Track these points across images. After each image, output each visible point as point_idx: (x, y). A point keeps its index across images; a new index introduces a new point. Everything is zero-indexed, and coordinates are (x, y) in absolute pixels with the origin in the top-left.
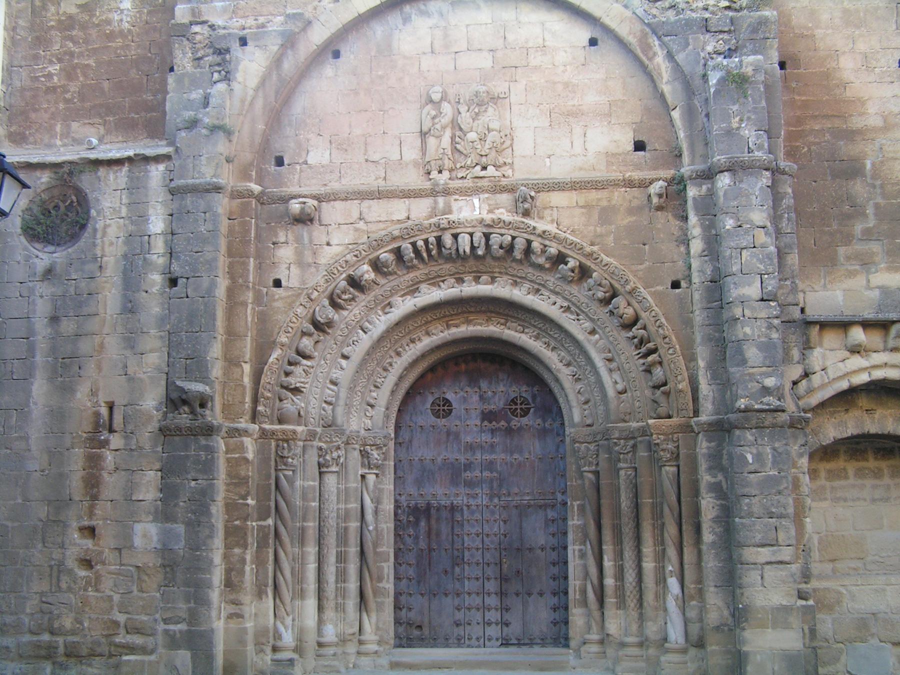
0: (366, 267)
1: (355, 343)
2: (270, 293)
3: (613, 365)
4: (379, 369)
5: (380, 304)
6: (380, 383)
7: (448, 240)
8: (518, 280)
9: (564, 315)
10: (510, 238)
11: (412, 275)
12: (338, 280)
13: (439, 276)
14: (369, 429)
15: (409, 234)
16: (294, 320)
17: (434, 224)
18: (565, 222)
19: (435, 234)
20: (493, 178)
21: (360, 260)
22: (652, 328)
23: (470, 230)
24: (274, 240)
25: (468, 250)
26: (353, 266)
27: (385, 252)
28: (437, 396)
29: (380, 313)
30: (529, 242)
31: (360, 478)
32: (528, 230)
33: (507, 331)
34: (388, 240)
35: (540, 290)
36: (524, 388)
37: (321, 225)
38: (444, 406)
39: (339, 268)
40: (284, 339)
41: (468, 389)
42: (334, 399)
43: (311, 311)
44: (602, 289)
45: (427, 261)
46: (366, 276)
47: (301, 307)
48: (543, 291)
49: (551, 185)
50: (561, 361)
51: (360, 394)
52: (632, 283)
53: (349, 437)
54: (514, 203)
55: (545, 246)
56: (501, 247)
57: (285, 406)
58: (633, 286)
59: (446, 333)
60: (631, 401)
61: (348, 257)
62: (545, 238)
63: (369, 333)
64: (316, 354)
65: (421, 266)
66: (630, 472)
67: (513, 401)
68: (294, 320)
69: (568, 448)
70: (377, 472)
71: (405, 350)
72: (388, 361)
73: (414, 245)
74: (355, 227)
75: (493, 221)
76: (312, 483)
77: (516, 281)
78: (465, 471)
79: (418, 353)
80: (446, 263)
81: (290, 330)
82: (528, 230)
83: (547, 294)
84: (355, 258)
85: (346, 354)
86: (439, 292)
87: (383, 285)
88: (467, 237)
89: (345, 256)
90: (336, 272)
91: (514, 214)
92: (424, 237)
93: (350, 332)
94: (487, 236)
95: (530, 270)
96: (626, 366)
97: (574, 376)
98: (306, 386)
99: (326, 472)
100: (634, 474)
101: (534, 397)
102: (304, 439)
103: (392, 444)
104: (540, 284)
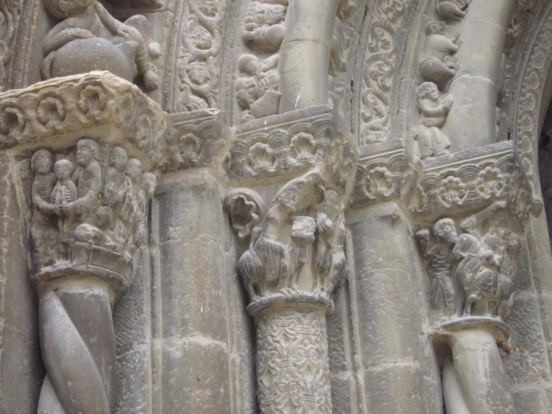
42: (282, 26)
51: (387, 37)
53: (360, 173)
57: (70, 31)
76: (204, 341)
99: (271, 305)
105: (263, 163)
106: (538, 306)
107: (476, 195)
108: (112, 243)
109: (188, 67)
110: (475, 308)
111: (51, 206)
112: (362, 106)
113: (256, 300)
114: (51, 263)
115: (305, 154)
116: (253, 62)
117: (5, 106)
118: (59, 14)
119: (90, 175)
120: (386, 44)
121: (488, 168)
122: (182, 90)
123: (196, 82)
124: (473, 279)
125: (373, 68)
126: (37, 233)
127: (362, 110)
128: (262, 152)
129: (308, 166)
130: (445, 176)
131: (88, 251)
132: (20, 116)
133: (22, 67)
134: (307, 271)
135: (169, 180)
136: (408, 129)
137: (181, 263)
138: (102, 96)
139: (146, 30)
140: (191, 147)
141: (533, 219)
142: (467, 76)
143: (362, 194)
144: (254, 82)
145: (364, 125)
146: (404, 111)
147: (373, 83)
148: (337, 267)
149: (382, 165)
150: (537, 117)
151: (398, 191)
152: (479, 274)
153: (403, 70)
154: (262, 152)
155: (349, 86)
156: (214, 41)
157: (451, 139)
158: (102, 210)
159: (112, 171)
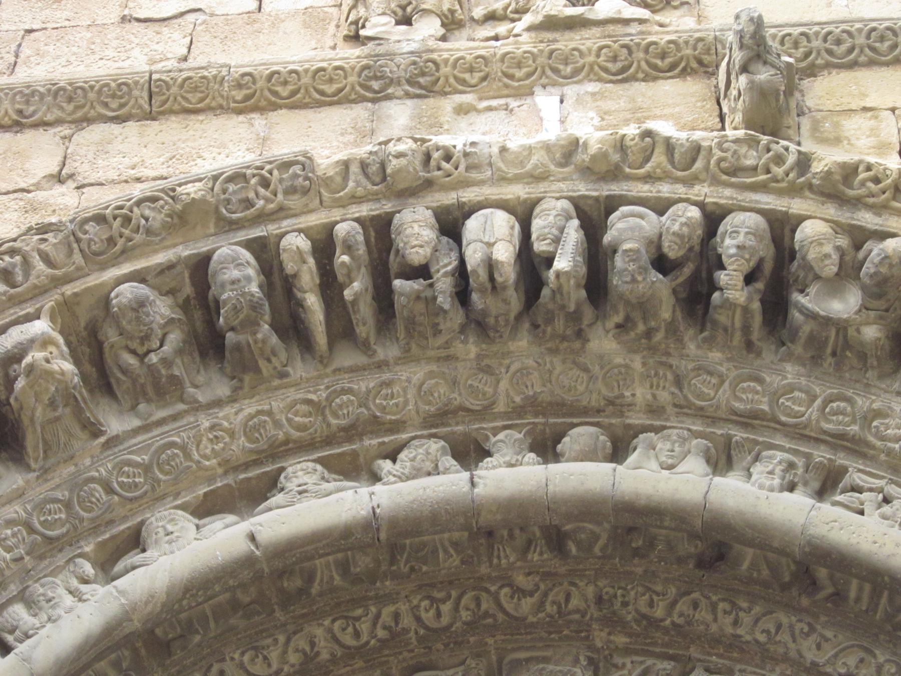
5: (96, 529)
8: (739, 434)
10: (694, 213)
11: (249, 407)
13: (376, 425)
15: (248, 204)
19: (364, 210)
20: (619, 29)
21: (18, 301)
23: (517, 192)
29: (88, 569)
32: (779, 171)
34: (157, 218)
35: (844, 470)
46: (35, 356)
49: (861, 40)
54: (711, 105)
62: (856, 203)
63: (21, 648)
65: (299, 370)
74: (30, 202)
77: (729, 438)
80: (406, 358)
92: (314, 220)
95: (792, 373)
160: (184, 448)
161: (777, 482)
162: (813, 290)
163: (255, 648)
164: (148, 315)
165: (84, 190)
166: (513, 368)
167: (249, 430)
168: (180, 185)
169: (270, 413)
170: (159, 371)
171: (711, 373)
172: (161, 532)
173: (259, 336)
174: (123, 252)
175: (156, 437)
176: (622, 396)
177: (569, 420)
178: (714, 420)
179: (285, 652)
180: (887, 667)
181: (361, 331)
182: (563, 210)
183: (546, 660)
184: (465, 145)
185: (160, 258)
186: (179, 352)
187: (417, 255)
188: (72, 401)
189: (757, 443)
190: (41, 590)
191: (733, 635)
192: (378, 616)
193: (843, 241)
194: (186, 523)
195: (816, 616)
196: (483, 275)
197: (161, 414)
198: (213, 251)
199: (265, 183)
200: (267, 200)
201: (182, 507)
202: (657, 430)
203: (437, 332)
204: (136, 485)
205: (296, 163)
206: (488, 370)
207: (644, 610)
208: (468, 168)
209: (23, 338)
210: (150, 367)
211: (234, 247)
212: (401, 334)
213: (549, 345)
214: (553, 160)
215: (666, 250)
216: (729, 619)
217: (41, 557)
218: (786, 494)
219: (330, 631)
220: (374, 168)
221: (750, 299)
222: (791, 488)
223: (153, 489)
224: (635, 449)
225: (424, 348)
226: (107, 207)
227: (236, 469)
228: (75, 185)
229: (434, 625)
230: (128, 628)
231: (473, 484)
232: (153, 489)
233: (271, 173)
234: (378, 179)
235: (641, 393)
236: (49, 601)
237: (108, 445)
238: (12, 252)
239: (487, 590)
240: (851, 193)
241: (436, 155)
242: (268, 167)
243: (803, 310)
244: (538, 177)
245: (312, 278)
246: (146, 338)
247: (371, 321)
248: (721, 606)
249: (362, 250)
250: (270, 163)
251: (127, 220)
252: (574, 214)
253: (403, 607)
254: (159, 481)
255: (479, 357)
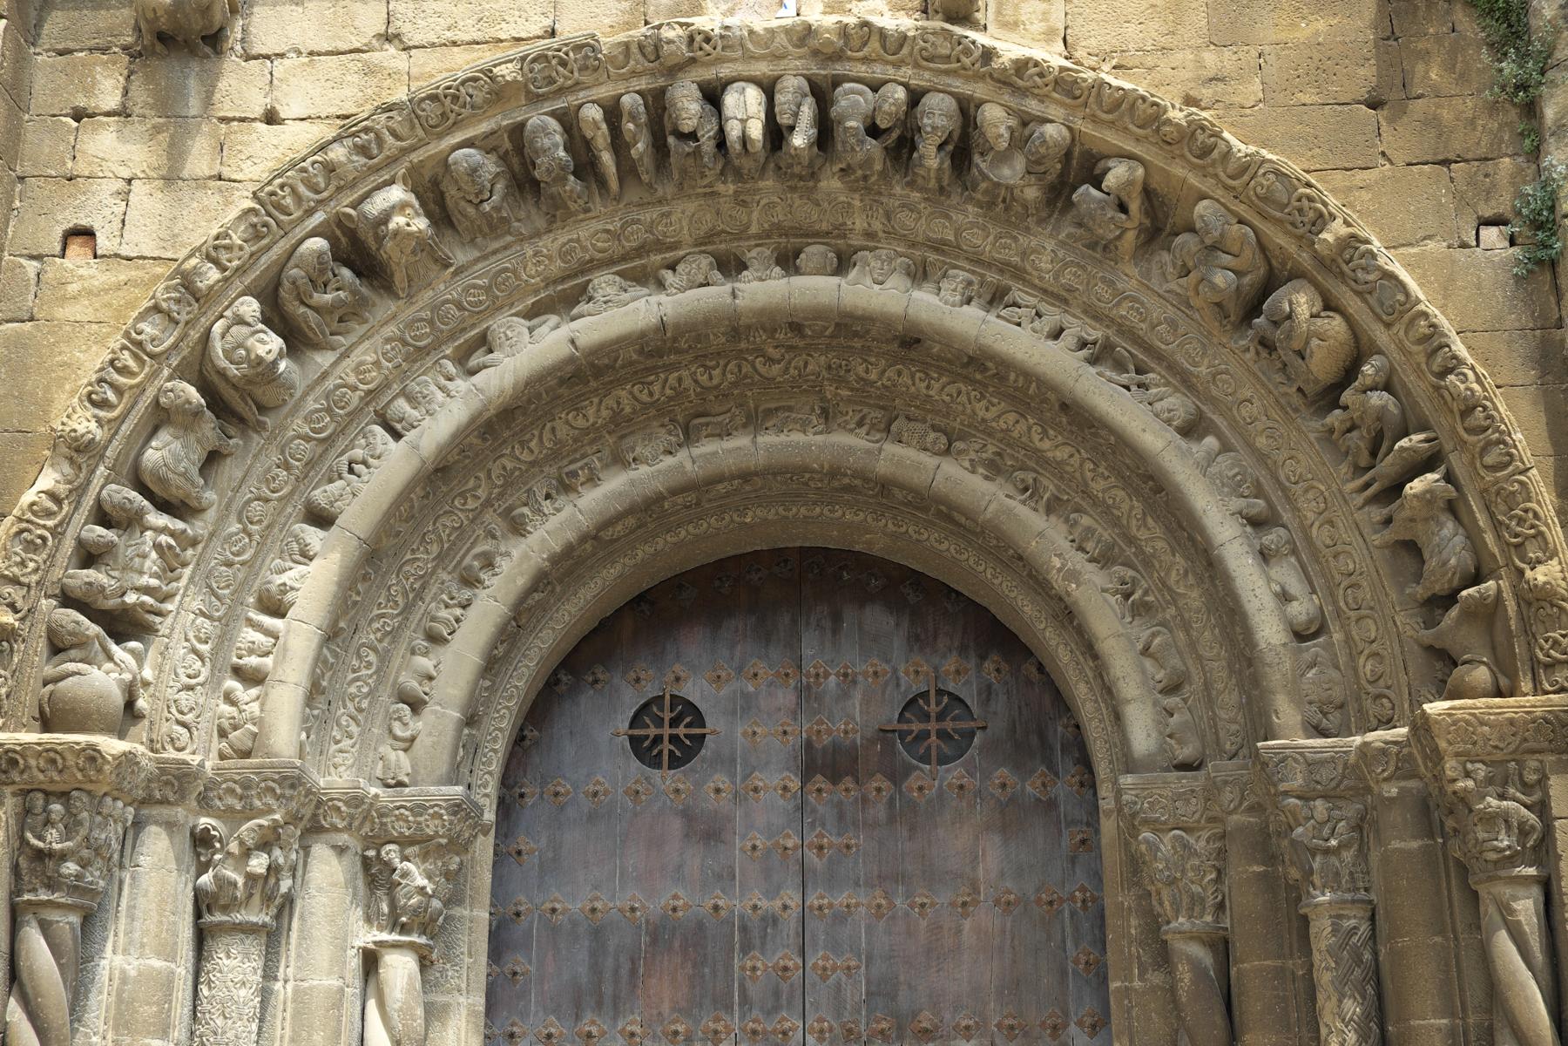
0: (396, 193)
1: (358, 468)
2: (49, 276)
3: (1272, 537)
4: (445, 576)
5: (452, 336)
6: (446, 622)
7: (688, 106)
8: (932, 257)
9: (1092, 370)
10: (901, 94)
12: (299, 232)
14: (400, 784)
15: (552, 81)
16: (127, 359)
17: (641, 47)
18: (1090, 40)
19: (643, 84)
21: (376, 169)
22: (1419, 387)
23: (762, 69)
24: (81, 102)
25: (756, 130)
26: (353, 185)
27: (468, 143)
28: (651, 691)
29: (450, 367)
30: (967, 110)
31: (354, 963)
32: (967, 61)
33: (891, 449)
34: (479, 97)
35: (1007, 290)
36: (950, 664)
37: (248, 58)
38: (674, 722)
39: (302, 189)
40: (85, 424)
41: (762, 668)
42: (268, 661)
43: (195, 335)
44: (1226, 259)
45: (614, 184)
46: (398, 221)
47: (157, 318)
48: (1017, 294)
50: (1081, 549)
51: (372, 657)
52: (1339, 221)
55: (1026, 121)
56: (873, 131)
58: (1344, 231)
59: (682, 455)
60: (1342, 660)
61: (338, 153)
62: (1024, 92)
63: (410, 436)
64: (210, 495)
65: (598, 206)
66: (1353, 922)
67: (911, 703)
68: (127, 359)
69: (1112, 857)
70: (423, 940)
71: (539, 511)
72: (478, 549)
73: (569, 121)
74: (366, 63)
75: (844, 30)
76: (157, 963)
78: (746, 949)
79: (585, 522)
81: (111, 396)
82: (967, 61)
83: (1032, 301)
84: (361, 160)
85: (323, 502)
86: (662, 298)
87: (459, 271)
88: (754, 96)
89: (322, 148)
90: (289, 201)
91: (917, 15)
92: (605, 91)
93: (342, 431)
94: (822, 93)
96: (1320, 535)
97: (1127, 596)
98: (169, 606)
100: (1364, 928)
101: (987, 693)
102: (141, 793)
103: (484, 848)
104: (1004, 267)
105: (230, 801)
106: (468, 924)
107: (422, 830)
108: (90, 879)
109: (176, 697)
110: (404, 929)
111: (41, 844)
112: (335, 728)
113: (208, 918)
114: (34, 890)
115: (270, 801)
116: (238, 693)
117: (7, 751)
118: (61, 645)
119: (80, 823)
120: (369, 664)
121: (436, 809)
122: (167, 720)
123: (182, 713)
124: (406, 904)
125: (353, 690)
126: (23, 863)
127: (334, 733)
128: (231, 791)
129: (271, 811)
130: (398, 808)
131: (69, 887)
132: (21, 762)
133: (22, 699)
134: (256, 899)
135: (145, 812)
136: (375, 749)
137: (147, 891)
138: (100, 761)
139: (139, 658)
140: (169, 787)
141: (481, 838)
142: (438, 708)
143: (319, 822)
144: (236, 714)
145: (334, 747)
146: (375, 731)
147: (350, 705)
148: (282, 896)
149: (340, 800)
150: (507, 733)
151: (350, 825)
152: (412, 901)
153: (381, 688)
154: (231, 791)
155: (326, 707)
156: (203, 669)
157: (412, 767)
158: (85, 853)
159: (99, 819)
160: (514, 272)
161: (958, 298)
162: (989, 158)
163: (577, 409)
164: (480, 177)
165: (413, 52)
166: (763, 202)
167: (563, 255)
168: (495, 66)
169: (578, 240)
170: (491, 216)
171: (912, 211)
172: (504, 338)
173: (567, 188)
174: (454, 124)
175: (493, 264)
176: (845, 224)
177: (805, 240)
178: (913, 245)
179: (598, 410)
180: (1035, 428)
181: (645, 178)
182: (799, 88)
183: (790, 409)
184: (721, 28)
185: (484, 127)
186: (504, 198)
187: (687, 126)
188: (428, 248)
189: (946, 263)
190: (418, 389)
191: (927, 396)
192: (666, 380)
193: (1013, 122)
194: (521, 325)
195: (985, 386)
196: (738, 147)
197: (496, 245)
198: (527, 120)
199: (563, 64)
200: (566, 78)
201: (516, 315)
202: (871, 250)
203: (703, 176)
204: (480, 302)
205: (588, 45)
206: (744, 203)
207: (863, 375)
208: (723, 48)
209: (386, 205)
210: (486, 216)
211: (543, 117)
212: (676, 176)
213: (789, 184)
214: (790, 41)
215: (878, 122)
216: (923, 385)
217: (415, 361)
218: (965, 307)
219: (631, 393)
220: (649, 49)
221: (942, 163)
222: (969, 301)
223: (494, 303)
224: (855, 265)
225: (693, 188)
226: (438, 88)
227: (555, 282)
228: (402, 47)
229: (709, 384)
230: (487, 415)
231: (734, 295)
232: (494, 303)
233: (567, 55)
234: (653, 58)
235: (859, 223)
236: (424, 397)
237: (455, 274)
238: (366, 130)
239: (746, 360)
240: (1020, 83)
241: (698, 38)
242: (565, 49)
243: (981, 172)
244: (777, 57)
245: (605, 140)
246: (481, 192)
247: (652, 168)
248: (918, 375)
249: (643, 119)
250: (566, 45)
251: (455, 98)
252: (807, 89)
253: (685, 373)
254: (497, 297)
255: (735, 192)
